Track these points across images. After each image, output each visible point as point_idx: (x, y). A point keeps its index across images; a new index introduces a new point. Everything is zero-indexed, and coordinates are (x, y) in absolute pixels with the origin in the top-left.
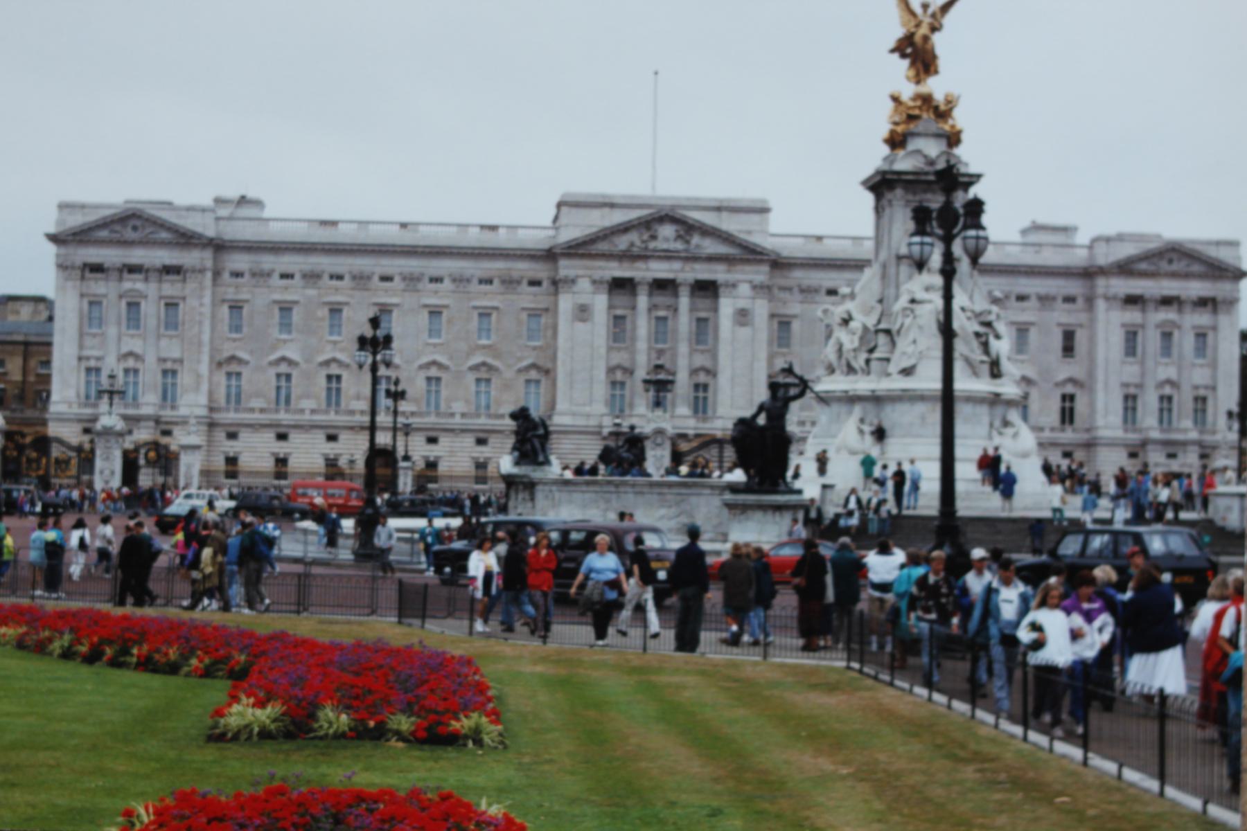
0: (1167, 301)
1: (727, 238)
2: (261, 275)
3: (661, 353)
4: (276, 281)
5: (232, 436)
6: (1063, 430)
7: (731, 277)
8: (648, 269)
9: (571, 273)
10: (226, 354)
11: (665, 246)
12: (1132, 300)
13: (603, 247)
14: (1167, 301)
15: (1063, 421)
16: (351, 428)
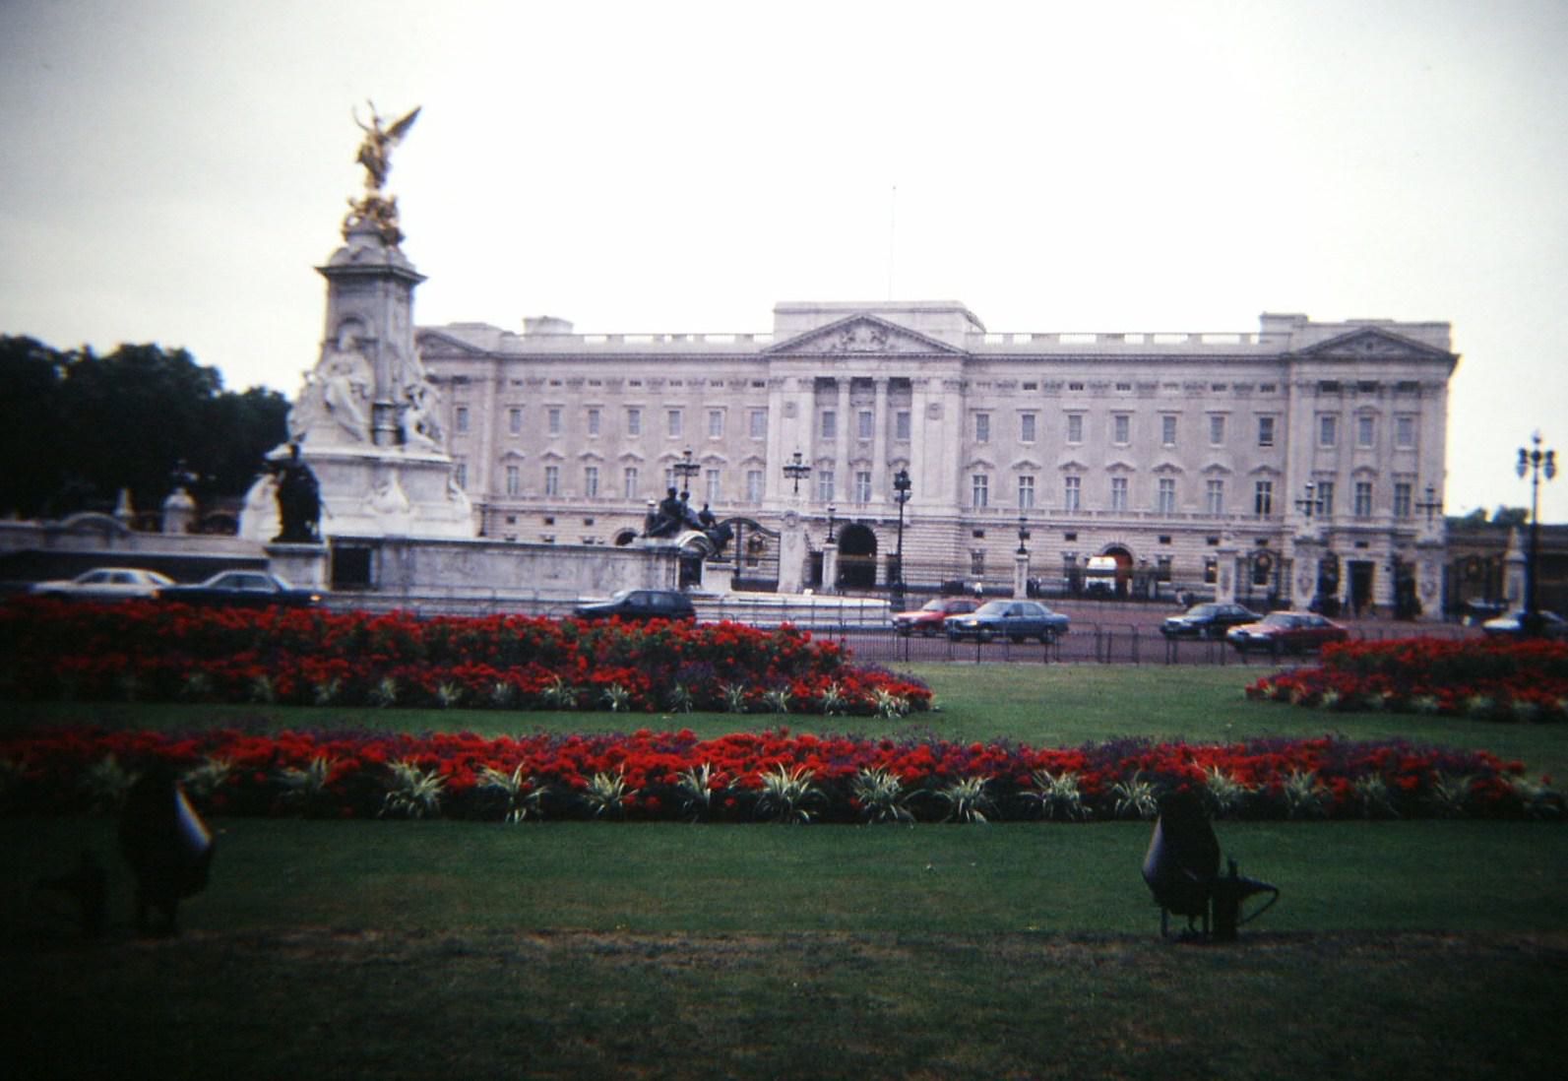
0: (1367, 387)
1: (919, 338)
2: (535, 383)
3: (864, 445)
4: (547, 387)
5: (511, 520)
6: (1257, 518)
7: (924, 374)
8: (848, 369)
9: (781, 374)
10: (505, 451)
11: (862, 347)
12: (1329, 387)
13: (809, 349)
14: (1367, 387)
15: (1258, 509)
16: (602, 514)
